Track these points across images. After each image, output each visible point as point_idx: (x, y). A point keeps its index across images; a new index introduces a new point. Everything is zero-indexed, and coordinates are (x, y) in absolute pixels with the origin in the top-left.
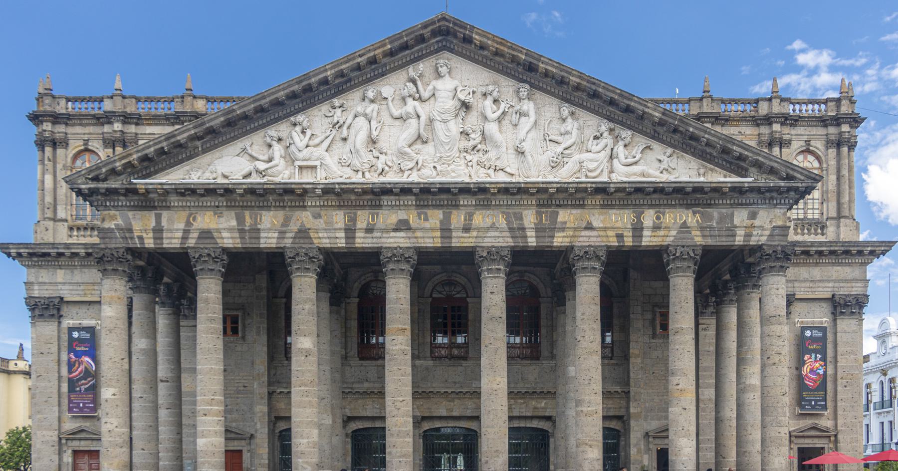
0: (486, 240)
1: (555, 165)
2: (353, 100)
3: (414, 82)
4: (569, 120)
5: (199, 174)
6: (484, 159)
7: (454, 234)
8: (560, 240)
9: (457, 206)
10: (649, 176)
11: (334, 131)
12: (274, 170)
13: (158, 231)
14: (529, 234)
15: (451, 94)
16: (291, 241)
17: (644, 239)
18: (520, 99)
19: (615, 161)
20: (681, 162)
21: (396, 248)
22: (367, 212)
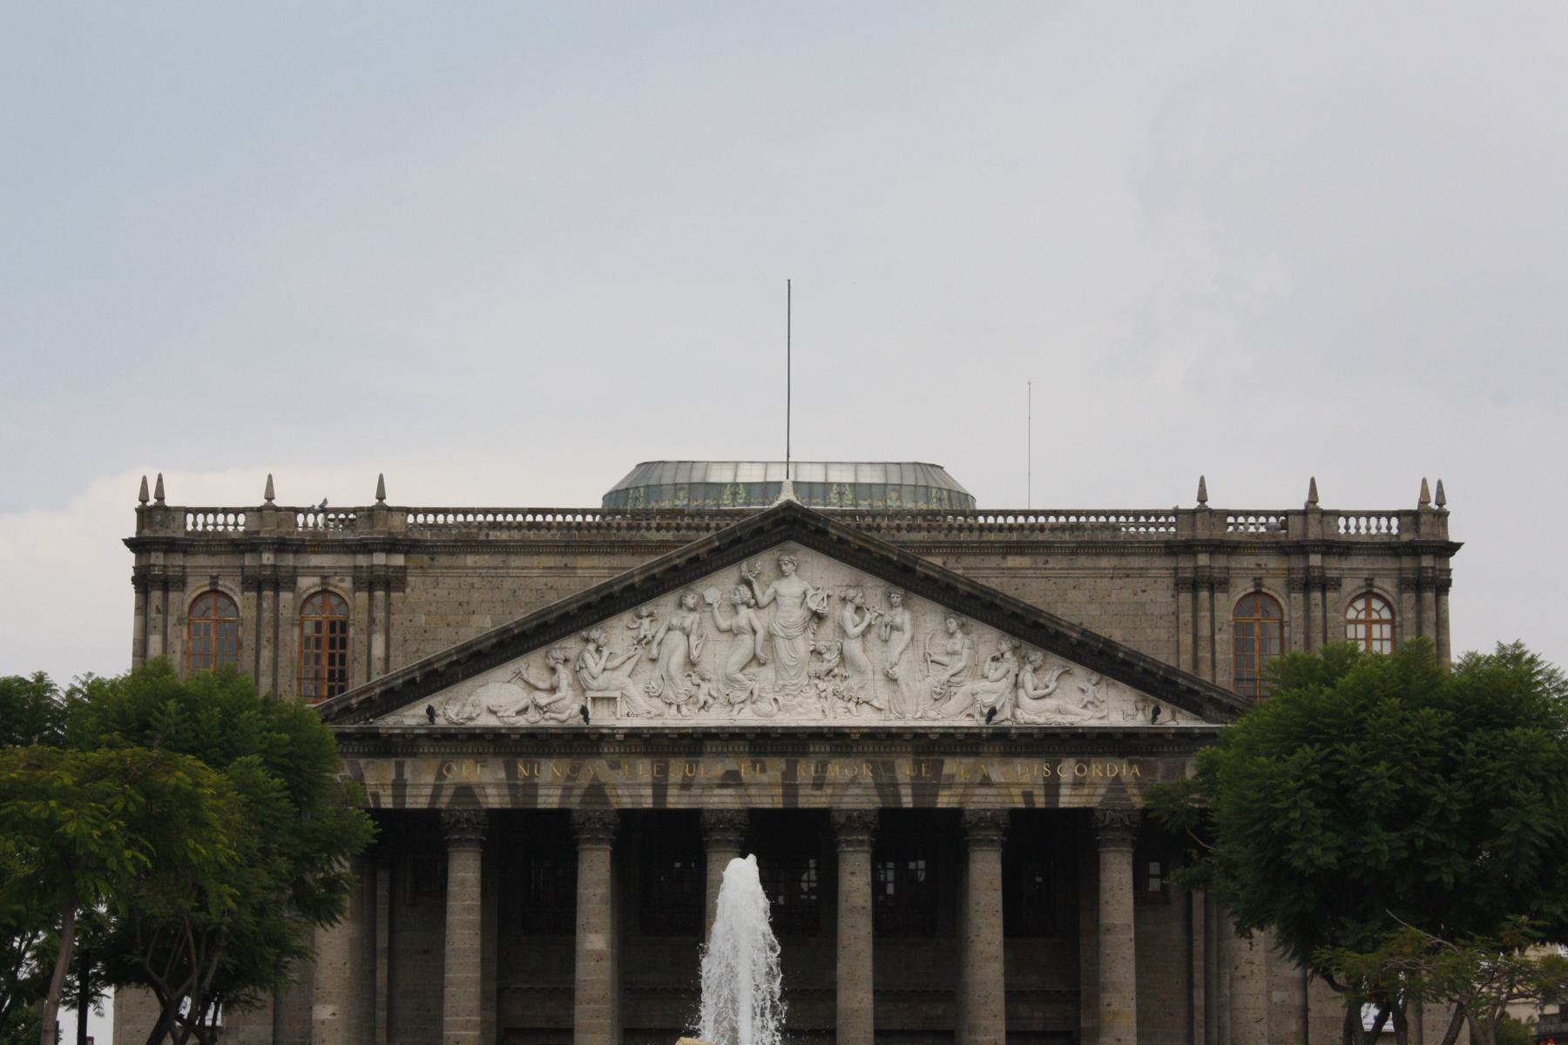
0: (846, 799)
1: (938, 697)
2: (665, 606)
3: (749, 584)
4: (959, 635)
5: (457, 708)
6: (842, 686)
7: (801, 792)
8: (945, 800)
9: (805, 754)
10: (1067, 713)
11: (640, 651)
12: (560, 704)
13: (399, 787)
15: (798, 601)
16: (578, 800)
17: (1061, 799)
18: (892, 606)
19: (1021, 692)
20: (1112, 691)
21: (721, 811)
22: (683, 760)
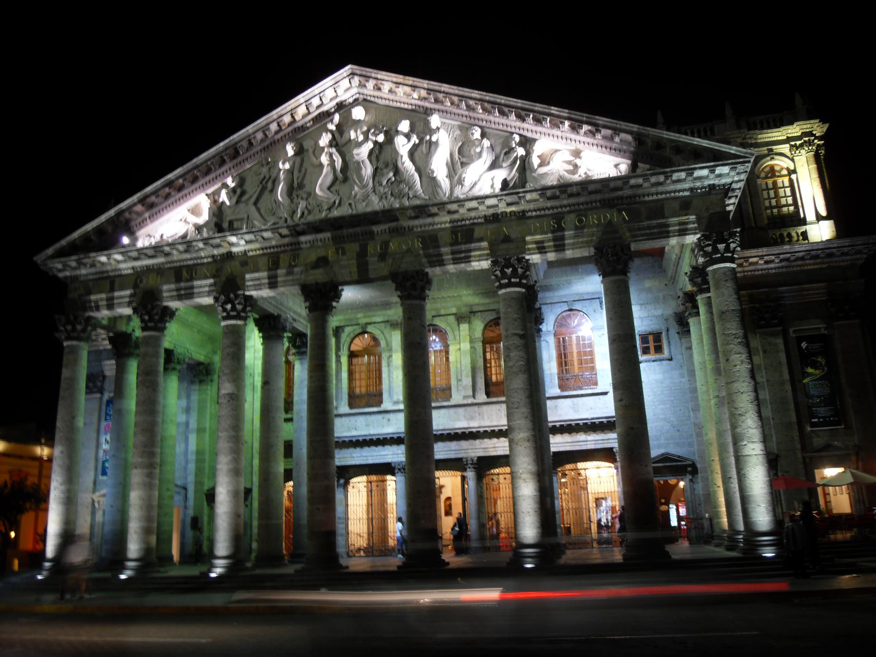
19: (528, 173)
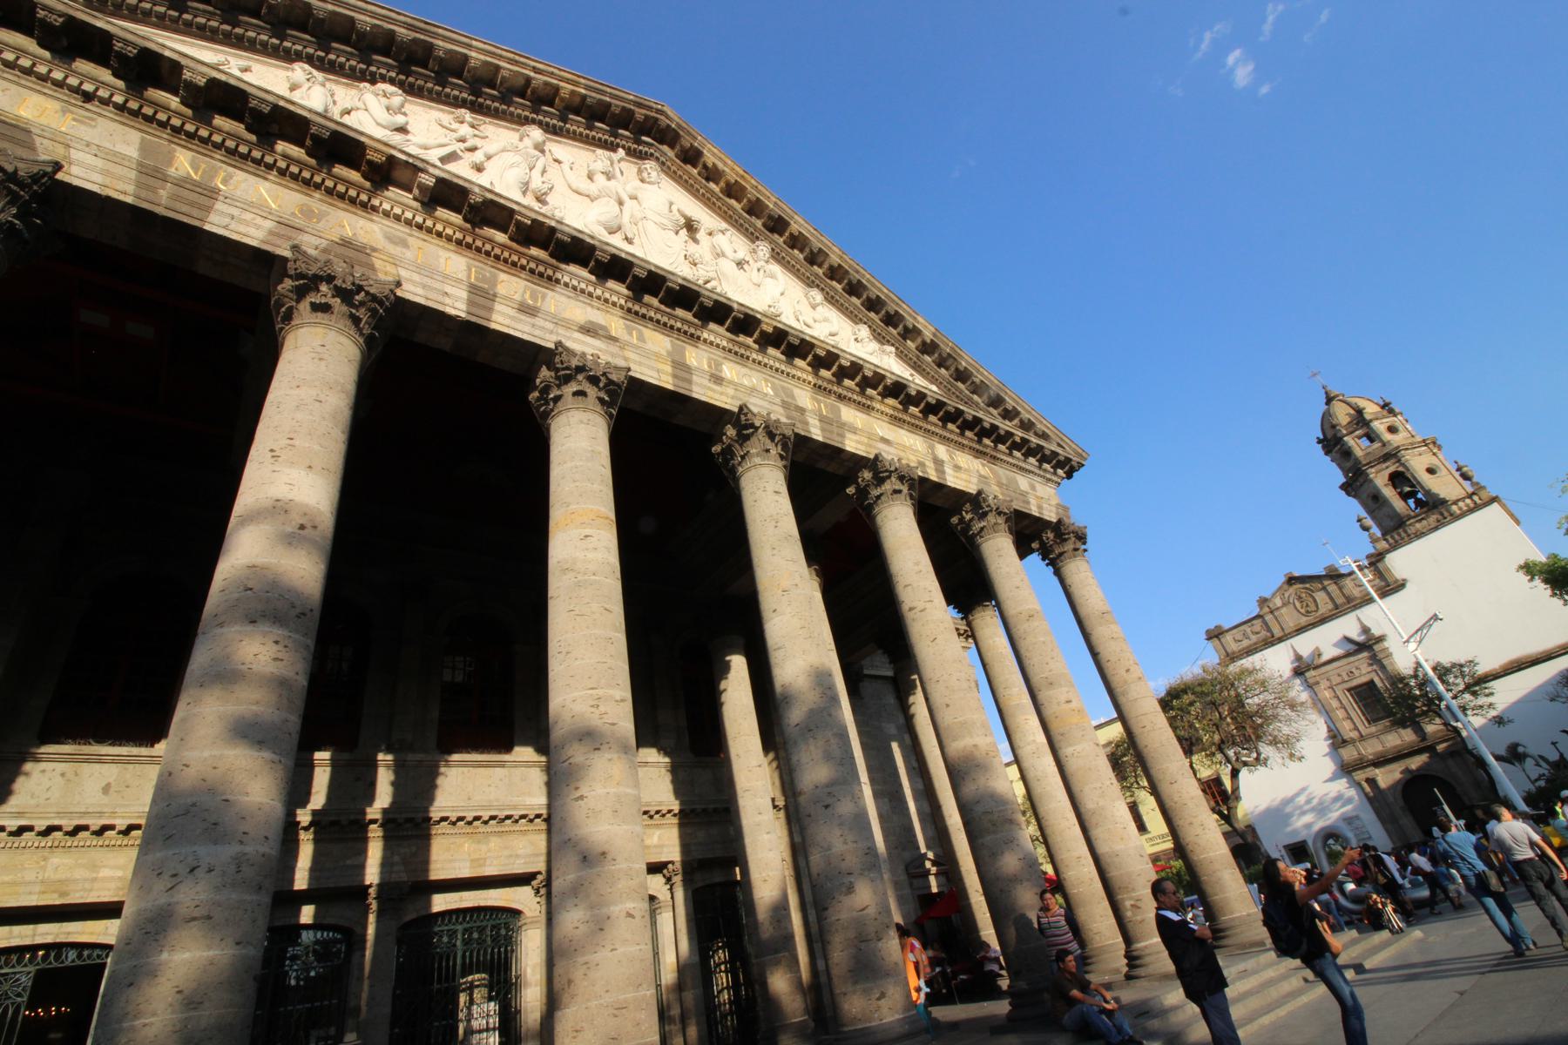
14: (811, 421)
